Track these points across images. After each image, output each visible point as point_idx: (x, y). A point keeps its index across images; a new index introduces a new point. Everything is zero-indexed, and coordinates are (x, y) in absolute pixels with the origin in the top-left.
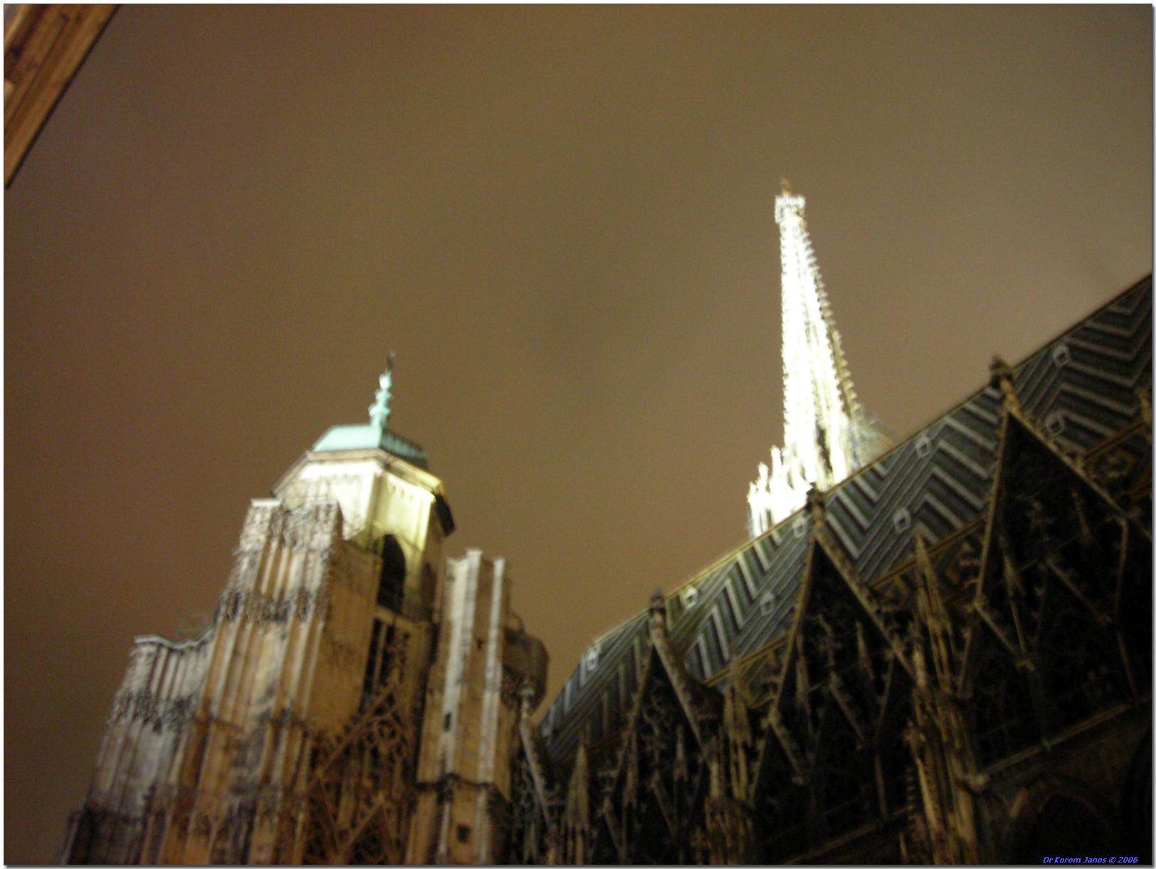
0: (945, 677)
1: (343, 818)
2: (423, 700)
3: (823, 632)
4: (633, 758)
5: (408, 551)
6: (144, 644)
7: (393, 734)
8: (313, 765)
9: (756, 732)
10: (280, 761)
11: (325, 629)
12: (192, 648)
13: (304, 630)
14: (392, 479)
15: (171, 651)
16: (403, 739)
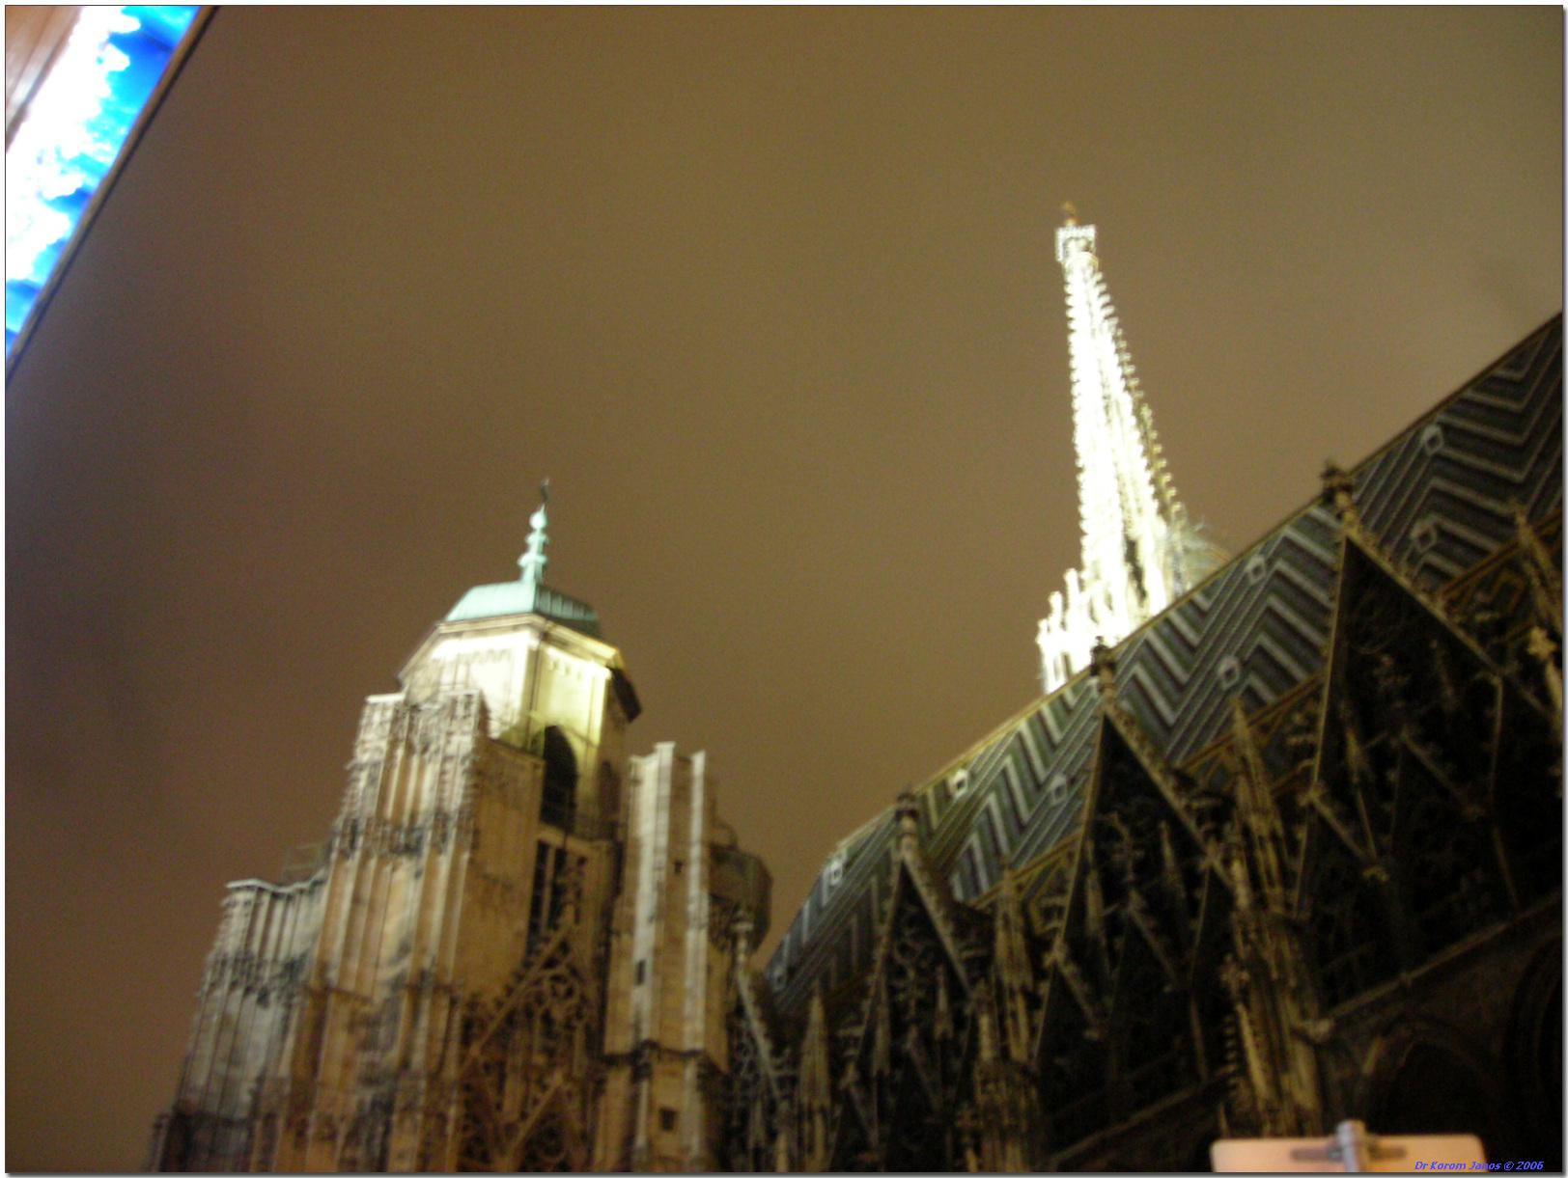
0: (1275, 892)
2: (607, 945)
3: (1118, 837)
4: (884, 1011)
5: (578, 747)
6: (238, 889)
7: (570, 993)
8: (466, 1040)
9: (1039, 973)
10: (421, 1040)
11: (471, 862)
12: (302, 891)
13: (444, 864)
14: (552, 652)
15: (275, 896)
16: (583, 998)
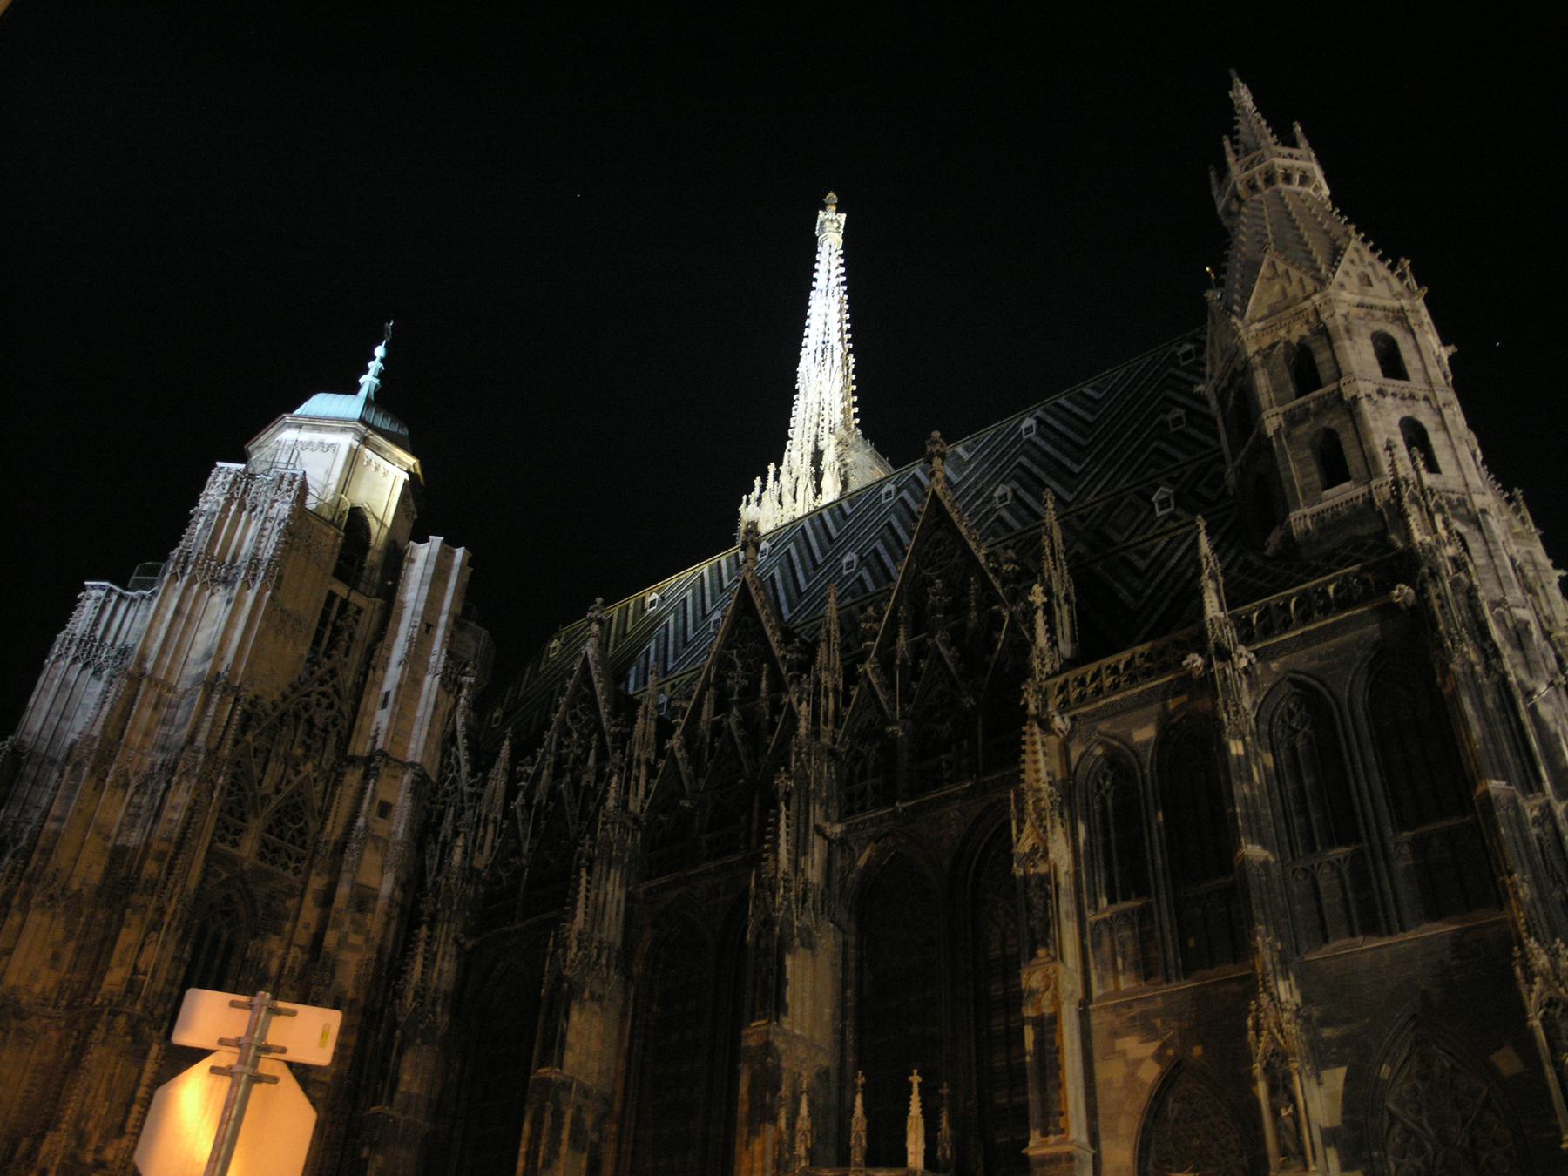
0: (827, 730)
1: (269, 782)
2: (366, 676)
3: (735, 669)
4: (552, 759)
5: (374, 527)
6: (93, 587)
7: (331, 706)
8: (244, 728)
9: (660, 753)
10: (207, 725)
11: (271, 598)
12: (143, 597)
13: (251, 596)
15: (121, 597)
16: (339, 711)
